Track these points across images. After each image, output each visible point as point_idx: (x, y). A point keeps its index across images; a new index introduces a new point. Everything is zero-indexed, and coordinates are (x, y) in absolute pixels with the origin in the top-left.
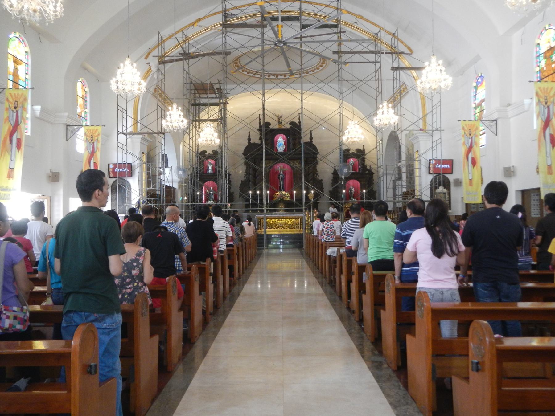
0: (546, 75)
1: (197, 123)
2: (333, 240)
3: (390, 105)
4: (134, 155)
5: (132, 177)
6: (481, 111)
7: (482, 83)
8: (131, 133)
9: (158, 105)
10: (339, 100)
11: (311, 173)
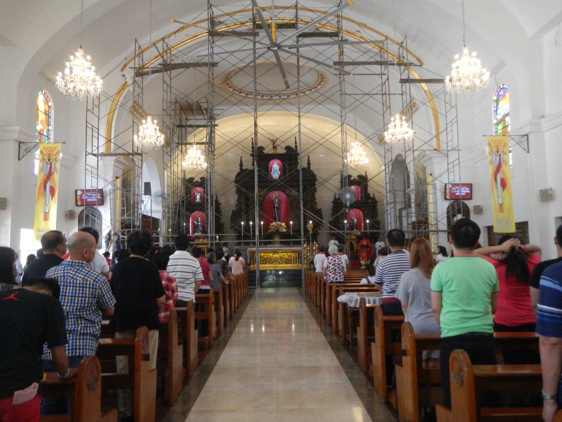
1: (183, 146)
2: (341, 280)
3: (404, 118)
4: (105, 180)
5: (103, 205)
6: (505, 127)
7: (504, 96)
8: (103, 155)
9: (133, 122)
10: (341, 117)
11: (309, 202)
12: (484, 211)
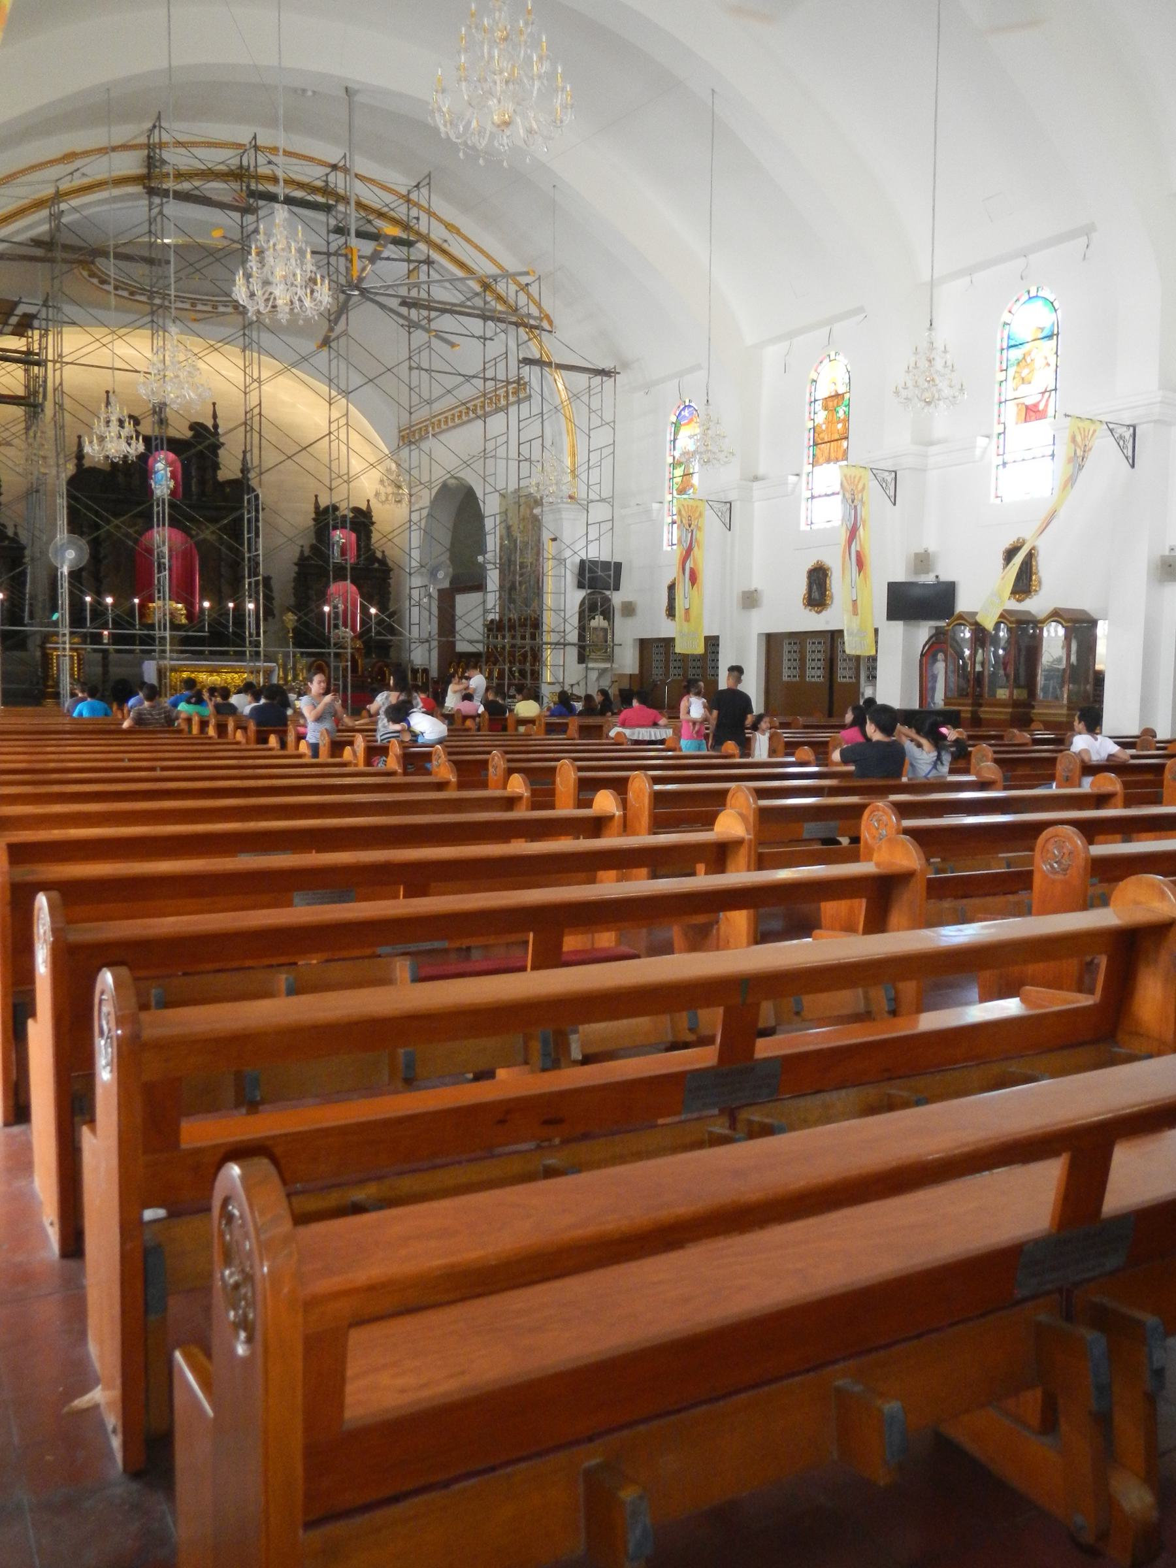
0: (826, 440)
12: (639, 611)
